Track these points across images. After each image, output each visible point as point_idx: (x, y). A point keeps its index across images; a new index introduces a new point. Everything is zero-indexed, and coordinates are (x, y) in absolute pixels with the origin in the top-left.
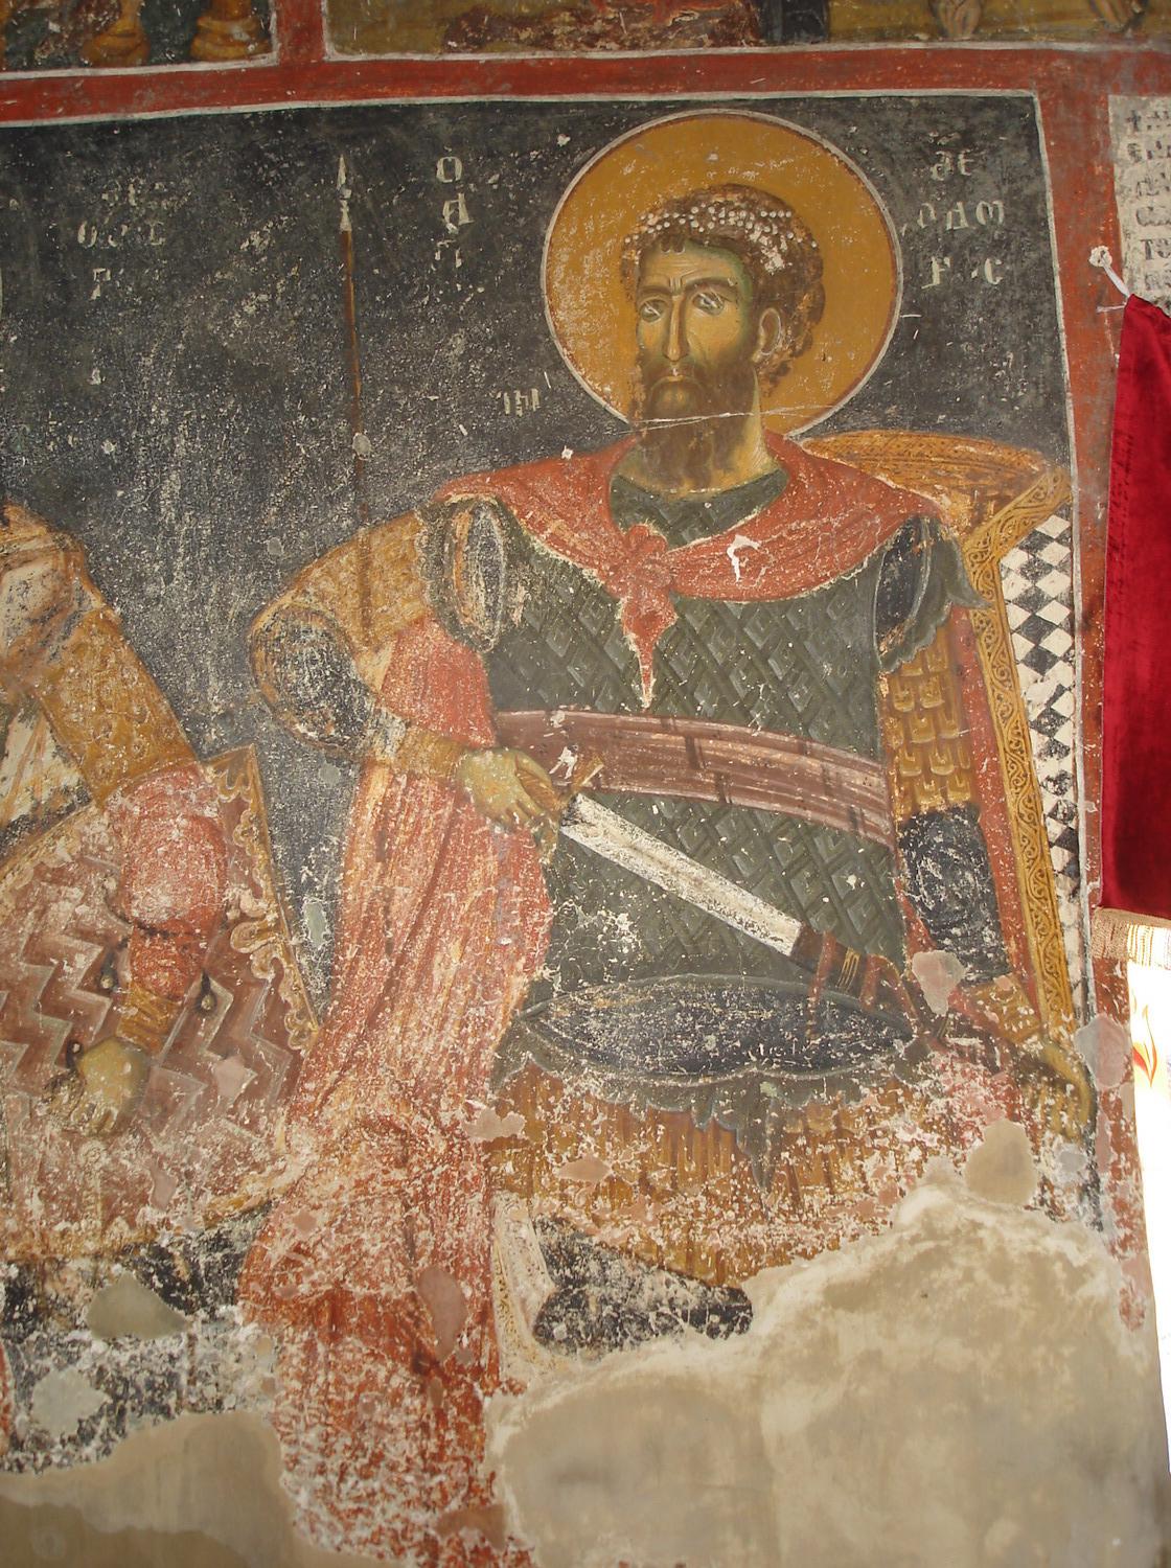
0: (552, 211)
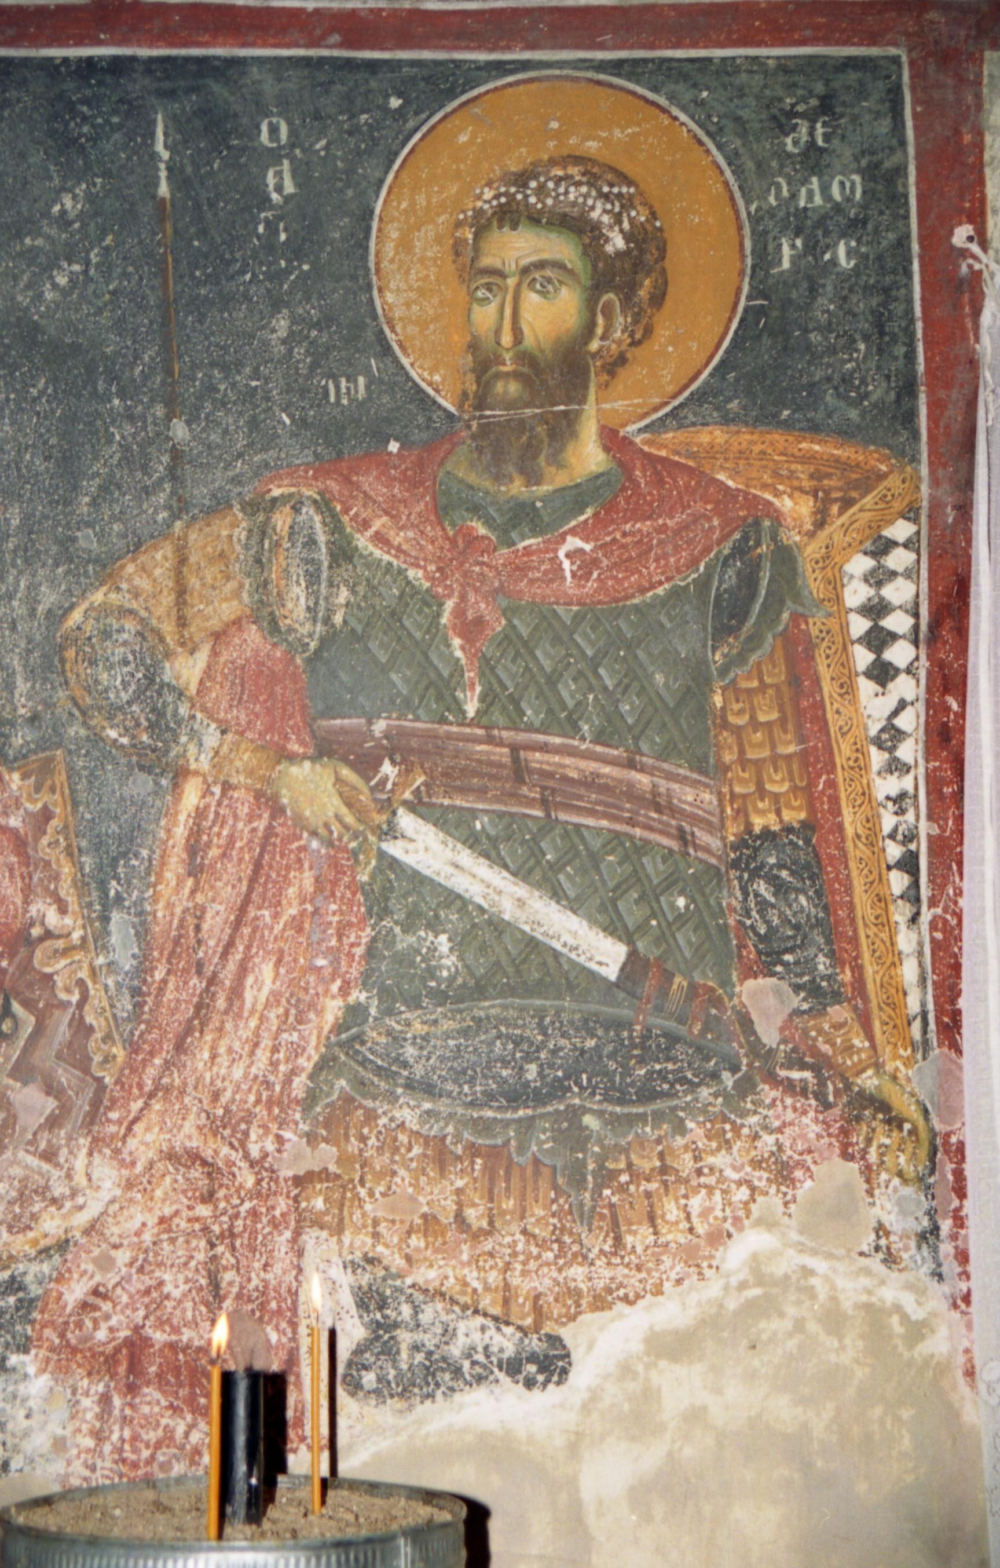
0: (381, 182)
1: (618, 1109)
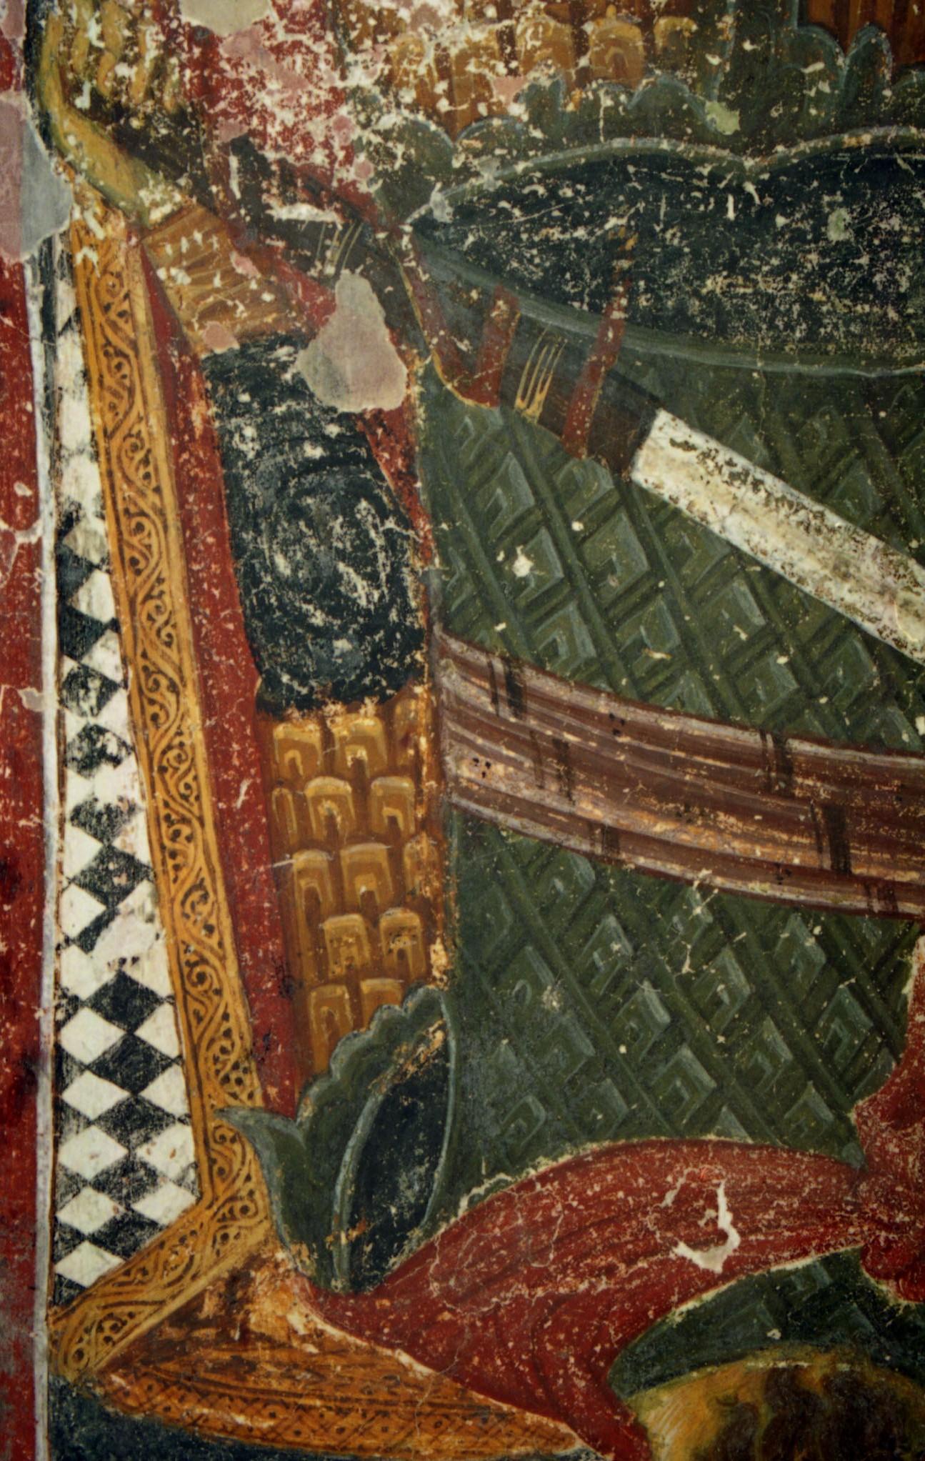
1: (665, 145)
